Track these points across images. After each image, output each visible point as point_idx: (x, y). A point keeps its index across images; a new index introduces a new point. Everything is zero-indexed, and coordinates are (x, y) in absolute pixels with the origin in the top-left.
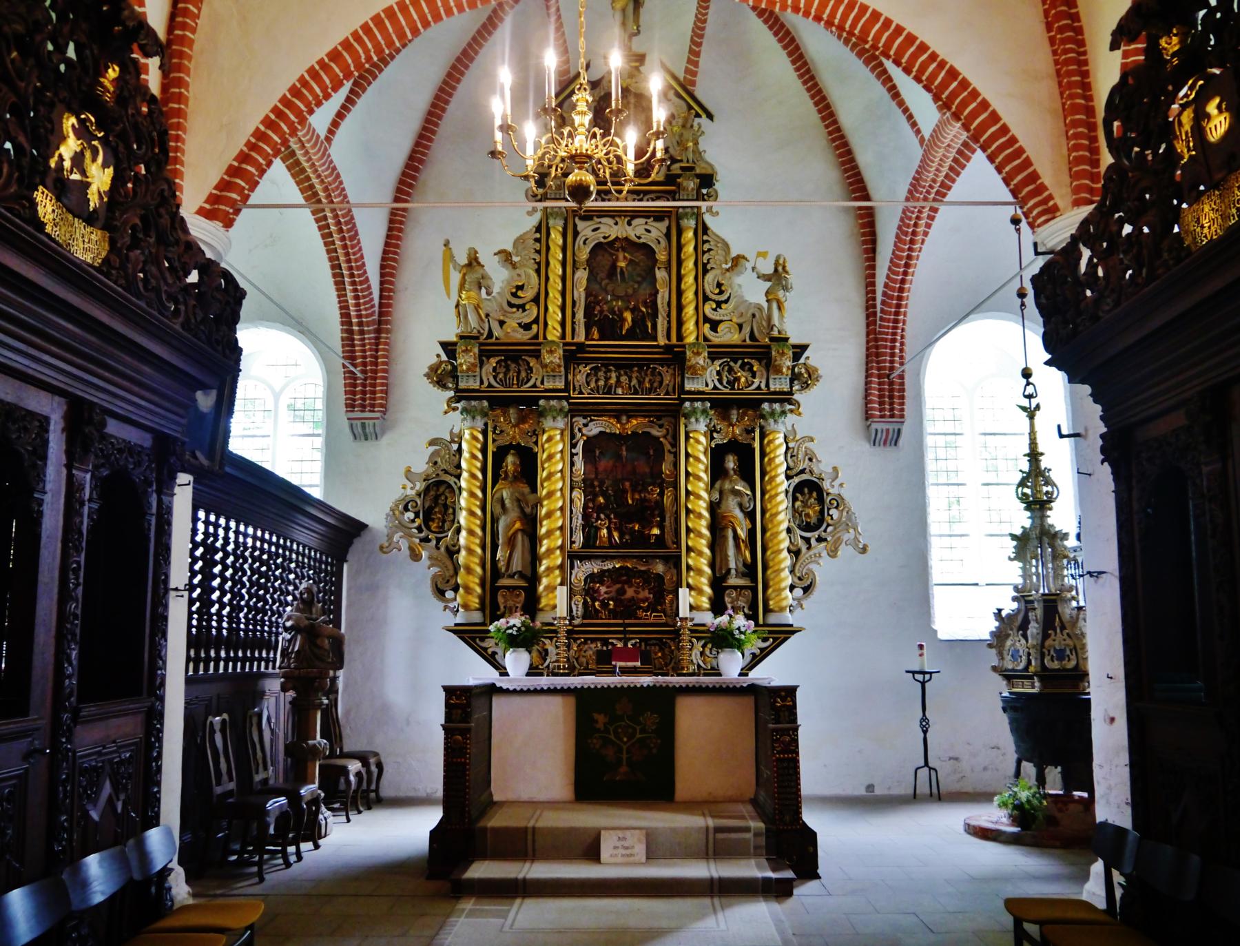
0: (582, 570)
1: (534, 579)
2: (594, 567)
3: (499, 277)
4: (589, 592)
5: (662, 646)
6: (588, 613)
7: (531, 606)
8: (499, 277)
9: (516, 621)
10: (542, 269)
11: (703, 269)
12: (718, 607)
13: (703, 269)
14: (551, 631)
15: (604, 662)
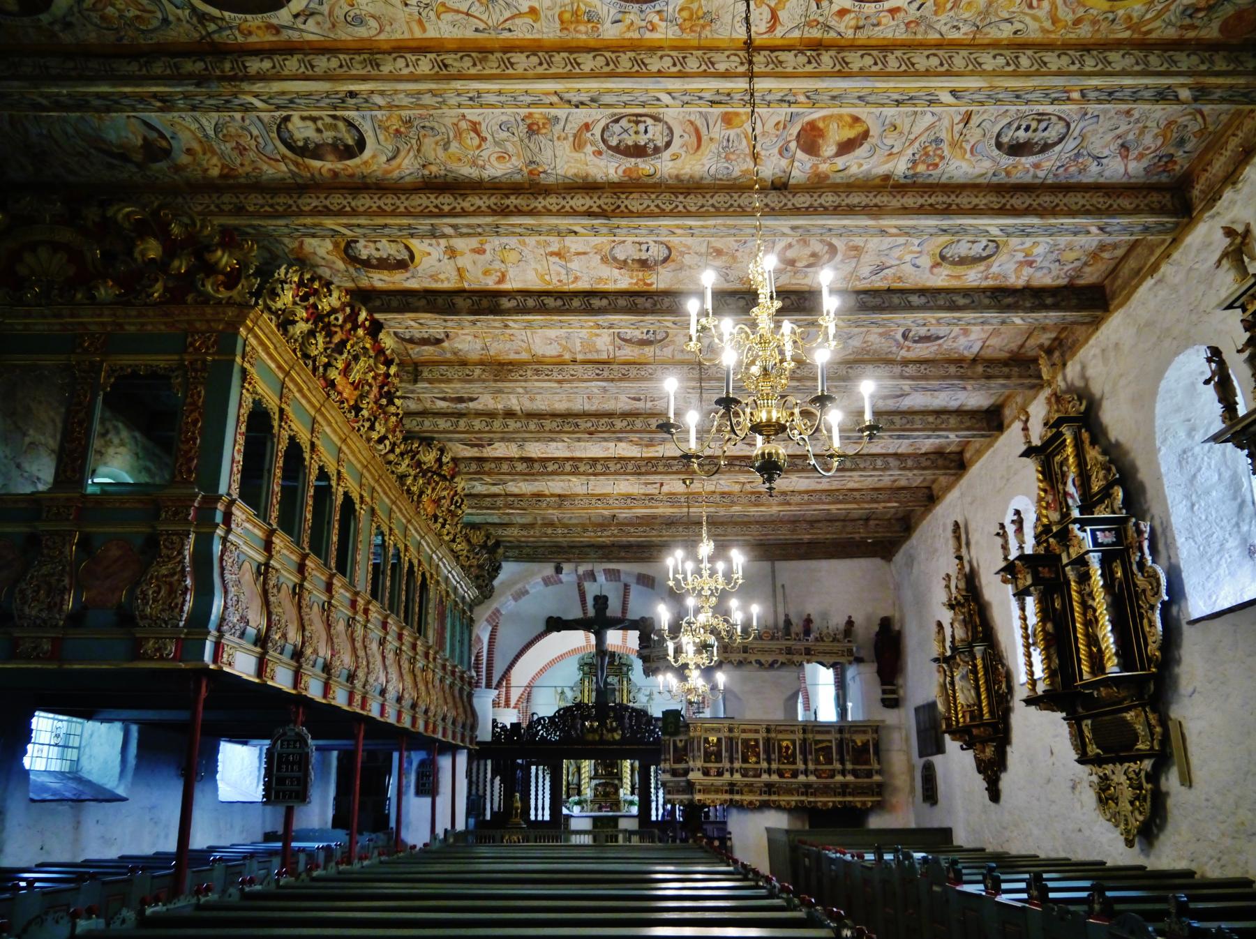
0: (594, 782)
1: (579, 785)
2: (597, 782)
3: (569, 694)
4: (596, 789)
5: (616, 805)
6: (595, 795)
7: (579, 793)
8: (569, 694)
9: (577, 798)
10: (582, 692)
11: (629, 692)
12: (632, 793)
13: (629, 692)
14: (586, 801)
15: (600, 809)
